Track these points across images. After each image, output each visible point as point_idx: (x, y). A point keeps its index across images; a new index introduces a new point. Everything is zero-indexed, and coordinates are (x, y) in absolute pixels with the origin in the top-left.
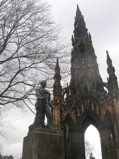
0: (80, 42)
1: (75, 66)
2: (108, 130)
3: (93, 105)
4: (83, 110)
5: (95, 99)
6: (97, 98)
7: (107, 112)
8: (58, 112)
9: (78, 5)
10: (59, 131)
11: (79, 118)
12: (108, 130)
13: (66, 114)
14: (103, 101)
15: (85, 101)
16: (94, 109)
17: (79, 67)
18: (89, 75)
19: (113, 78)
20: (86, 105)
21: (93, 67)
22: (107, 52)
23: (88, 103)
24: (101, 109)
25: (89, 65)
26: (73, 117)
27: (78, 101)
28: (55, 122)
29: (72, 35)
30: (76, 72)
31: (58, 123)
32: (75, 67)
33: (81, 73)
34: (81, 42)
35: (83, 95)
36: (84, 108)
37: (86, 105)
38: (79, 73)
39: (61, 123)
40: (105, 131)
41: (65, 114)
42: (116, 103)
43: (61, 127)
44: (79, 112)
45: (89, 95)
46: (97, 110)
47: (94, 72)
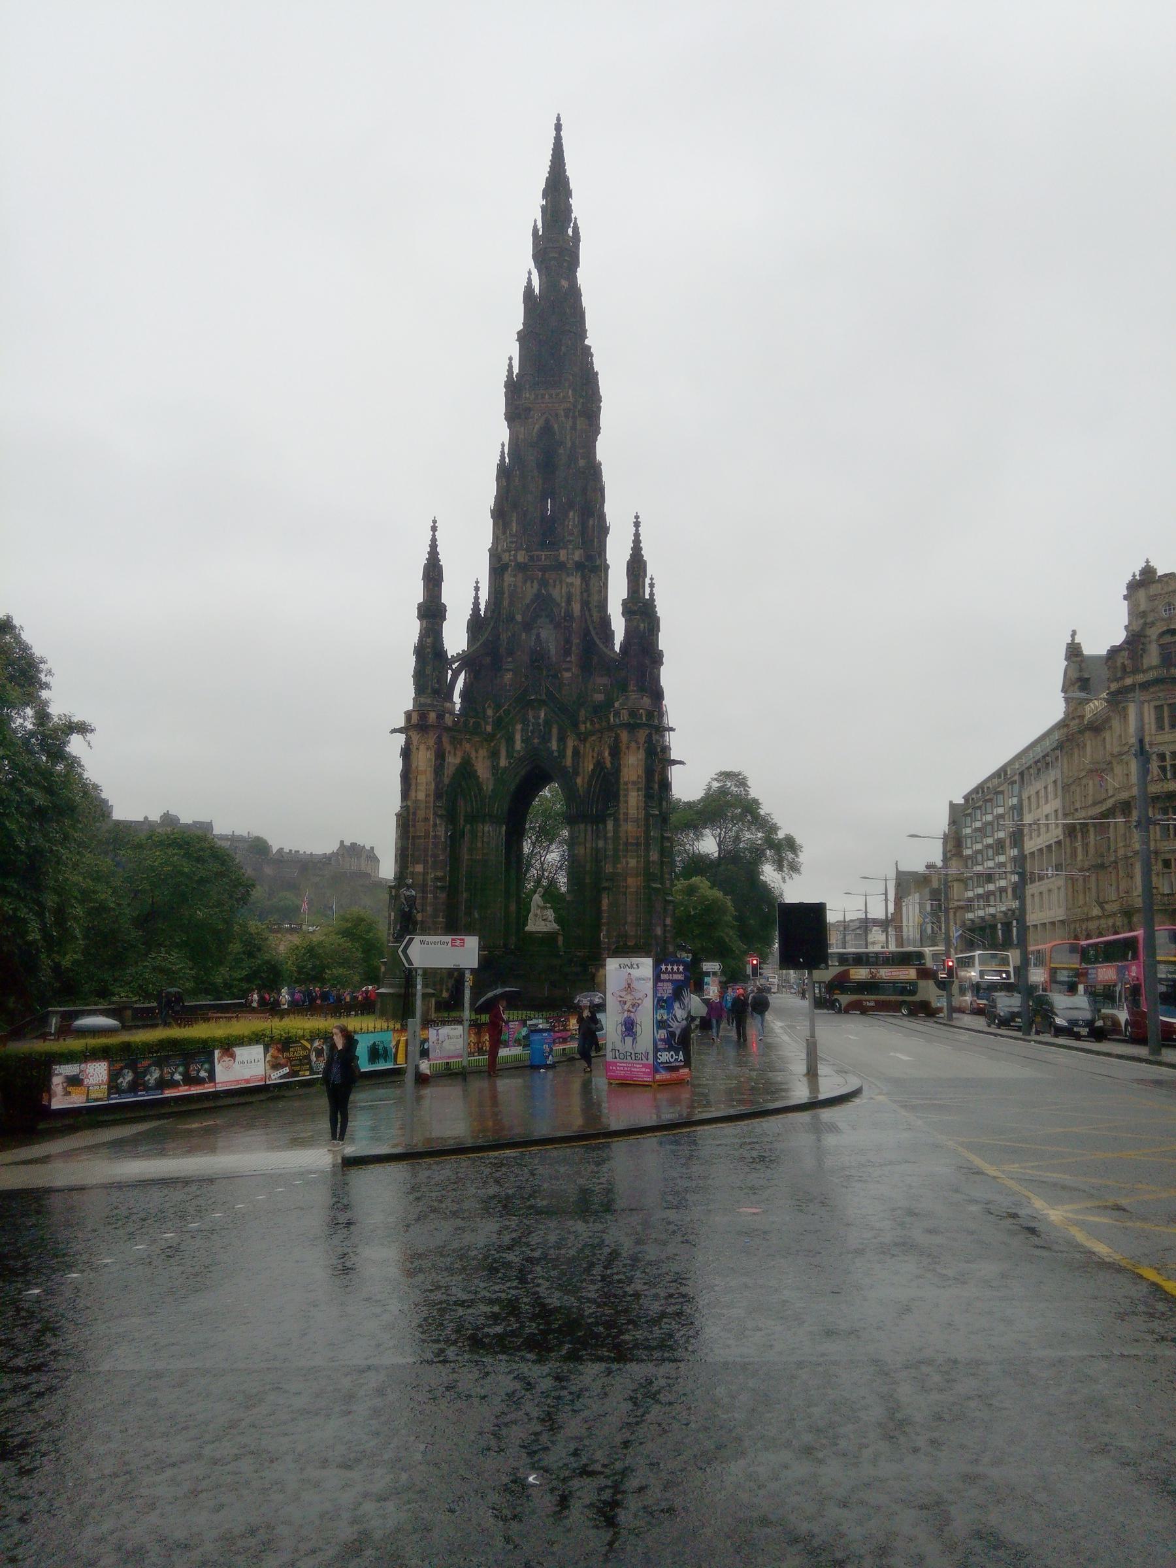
0: (542, 421)
3: (555, 731)
4: (518, 745)
9: (558, 127)
13: (458, 761)
15: (531, 714)
17: (521, 557)
18: (558, 599)
20: (531, 728)
22: (637, 525)
25: (563, 555)
26: (482, 769)
29: (511, 359)
30: (508, 579)
31: (427, 796)
32: (506, 557)
33: (529, 584)
34: (547, 421)
36: (523, 741)
37: (531, 728)
40: (586, 830)
41: (453, 761)
46: (569, 752)
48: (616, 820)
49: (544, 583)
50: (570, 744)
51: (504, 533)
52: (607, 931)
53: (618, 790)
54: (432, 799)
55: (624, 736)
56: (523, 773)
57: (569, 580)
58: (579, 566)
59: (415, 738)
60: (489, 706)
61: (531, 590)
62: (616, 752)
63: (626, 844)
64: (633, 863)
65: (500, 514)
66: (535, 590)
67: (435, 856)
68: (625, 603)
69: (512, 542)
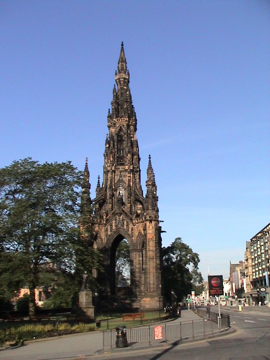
0: (119, 127)
1: (110, 166)
3: (125, 223)
4: (114, 228)
7: (140, 233)
9: (122, 45)
11: (109, 237)
14: (137, 220)
15: (117, 217)
16: (127, 228)
18: (125, 182)
19: (150, 195)
20: (118, 222)
21: (132, 171)
23: (121, 220)
24: (134, 228)
25: (127, 167)
29: (109, 109)
30: (109, 175)
32: (109, 168)
33: (116, 176)
34: (121, 127)
36: (115, 226)
38: (113, 177)
40: (136, 254)
42: (149, 228)
44: (109, 230)
46: (130, 230)
47: (131, 178)
48: (146, 251)
49: (121, 176)
50: (131, 226)
55: (148, 223)
57: (129, 175)
58: (132, 171)
61: (117, 178)
62: (145, 230)
65: (106, 155)
66: (118, 179)
68: (147, 182)
69: (110, 164)
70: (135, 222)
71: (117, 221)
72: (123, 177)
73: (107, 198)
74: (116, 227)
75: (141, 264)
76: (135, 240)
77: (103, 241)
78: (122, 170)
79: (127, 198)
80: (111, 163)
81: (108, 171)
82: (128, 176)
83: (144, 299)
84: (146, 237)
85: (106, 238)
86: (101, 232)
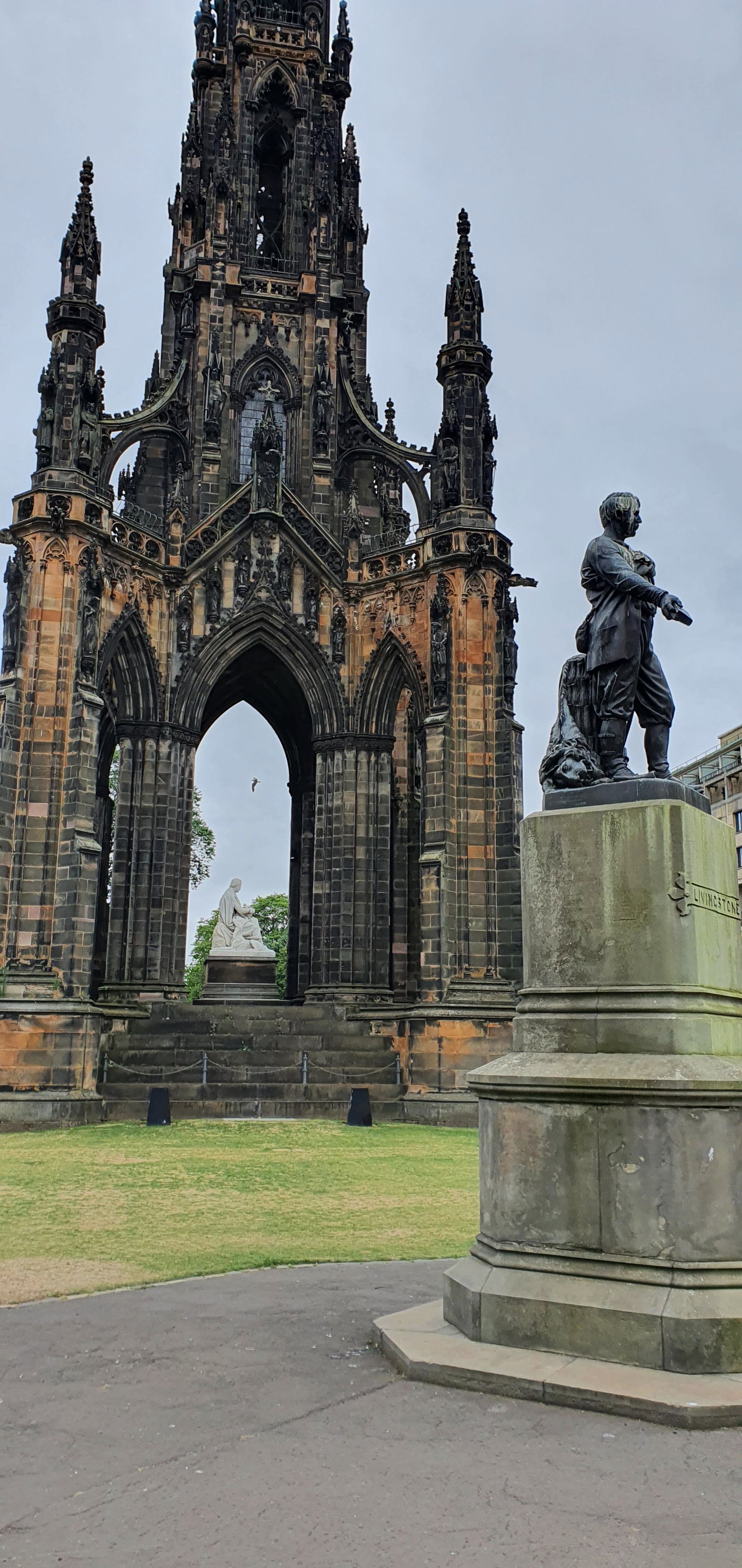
2: (373, 759)
3: (299, 580)
4: (229, 600)
5: (322, 545)
6: (333, 541)
8: (68, 584)
10: (69, 718)
12: (373, 759)
14: (371, 571)
15: (254, 543)
16: (307, 608)
17: (232, 275)
18: (294, 362)
19: (469, 422)
21: (336, 307)
23: (274, 558)
25: (307, 286)
27: (205, 532)
28: (37, 652)
30: (208, 309)
32: (204, 273)
33: (240, 329)
35: (244, 501)
36: (238, 592)
37: (254, 569)
38: (228, 323)
39: (85, 667)
40: (357, 762)
41: (111, 608)
43: (88, 695)
44: (199, 612)
45: (288, 505)
46: (326, 621)
51: (199, 235)
52: (438, 946)
53: (449, 677)
54: (72, 670)
56: (233, 653)
57: (324, 323)
58: (336, 307)
59: (39, 544)
60: (177, 521)
61: (246, 339)
62: (440, 612)
63: (465, 780)
64: (477, 816)
66: (253, 340)
67: (77, 784)
70: (360, 576)
71: (254, 561)
72: (281, 344)
73: (184, 433)
74: (239, 599)
75: (383, 820)
76: (357, 681)
77: (162, 670)
78: (276, 295)
79: (309, 447)
80: (223, 243)
81: (202, 290)
82: (319, 331)
83: (445, 1029)
84: (448, 655)
85: (177, 655)
86: (149, 612)
